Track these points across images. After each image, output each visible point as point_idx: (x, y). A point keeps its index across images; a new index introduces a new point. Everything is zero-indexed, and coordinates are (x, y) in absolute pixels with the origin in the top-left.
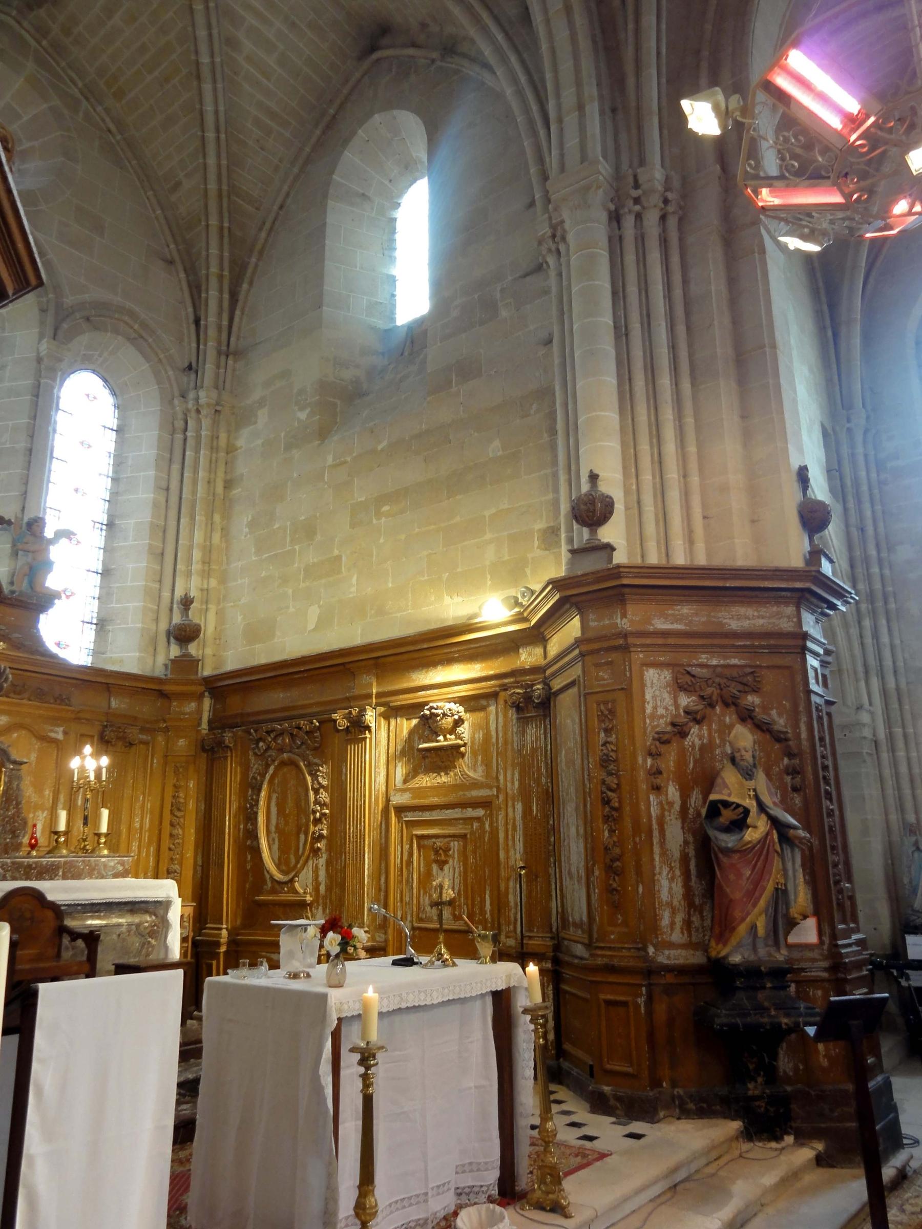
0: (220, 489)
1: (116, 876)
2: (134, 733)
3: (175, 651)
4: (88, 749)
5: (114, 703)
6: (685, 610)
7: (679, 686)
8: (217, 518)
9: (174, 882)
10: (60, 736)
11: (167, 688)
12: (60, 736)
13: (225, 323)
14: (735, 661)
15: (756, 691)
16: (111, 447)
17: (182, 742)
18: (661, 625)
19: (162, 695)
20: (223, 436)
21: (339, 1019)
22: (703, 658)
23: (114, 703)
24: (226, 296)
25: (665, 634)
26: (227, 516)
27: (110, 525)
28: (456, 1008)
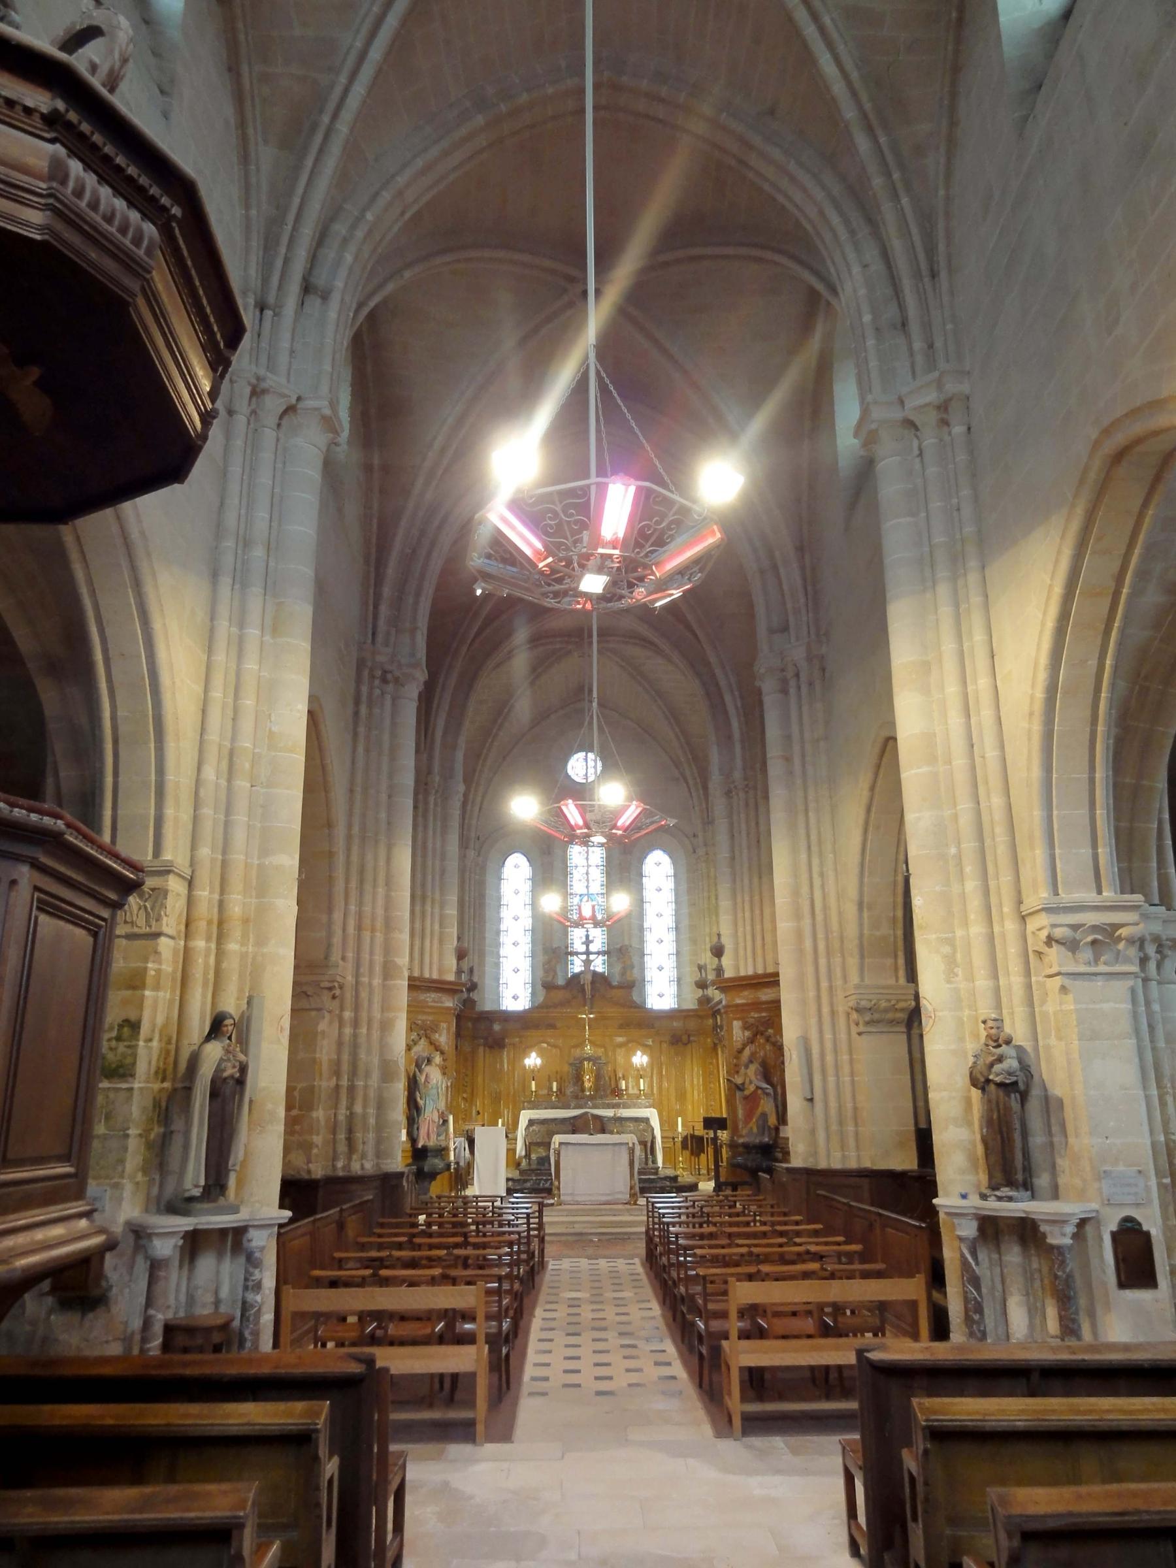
0: (713, 898)
1: (646, 1107)
2: (685, 1038)
3: (700, 992)
4: (639, 1053)
5: (675, 1024)
6: (746, 993)
7: (746, 1027)
8: (714, 918)
9: (655, 1110)
10: (651, 1043)
11: (700, 1013)
12: (651, 1043)
13: (704, 806)
14: (764, 1014)
15: (772, 1028)
16: (672, 885)
17: (709, 1040)
18: (739, 1001)
19: (700, 1017)
20: (712, 870)
21: (560, 1144)
22: (752, 1014)
23: (675, 1024)
24: (701, 792)
25: (737, 1005)
26: (717, 915)
27: (677, 928)
28: (610, 1147)
